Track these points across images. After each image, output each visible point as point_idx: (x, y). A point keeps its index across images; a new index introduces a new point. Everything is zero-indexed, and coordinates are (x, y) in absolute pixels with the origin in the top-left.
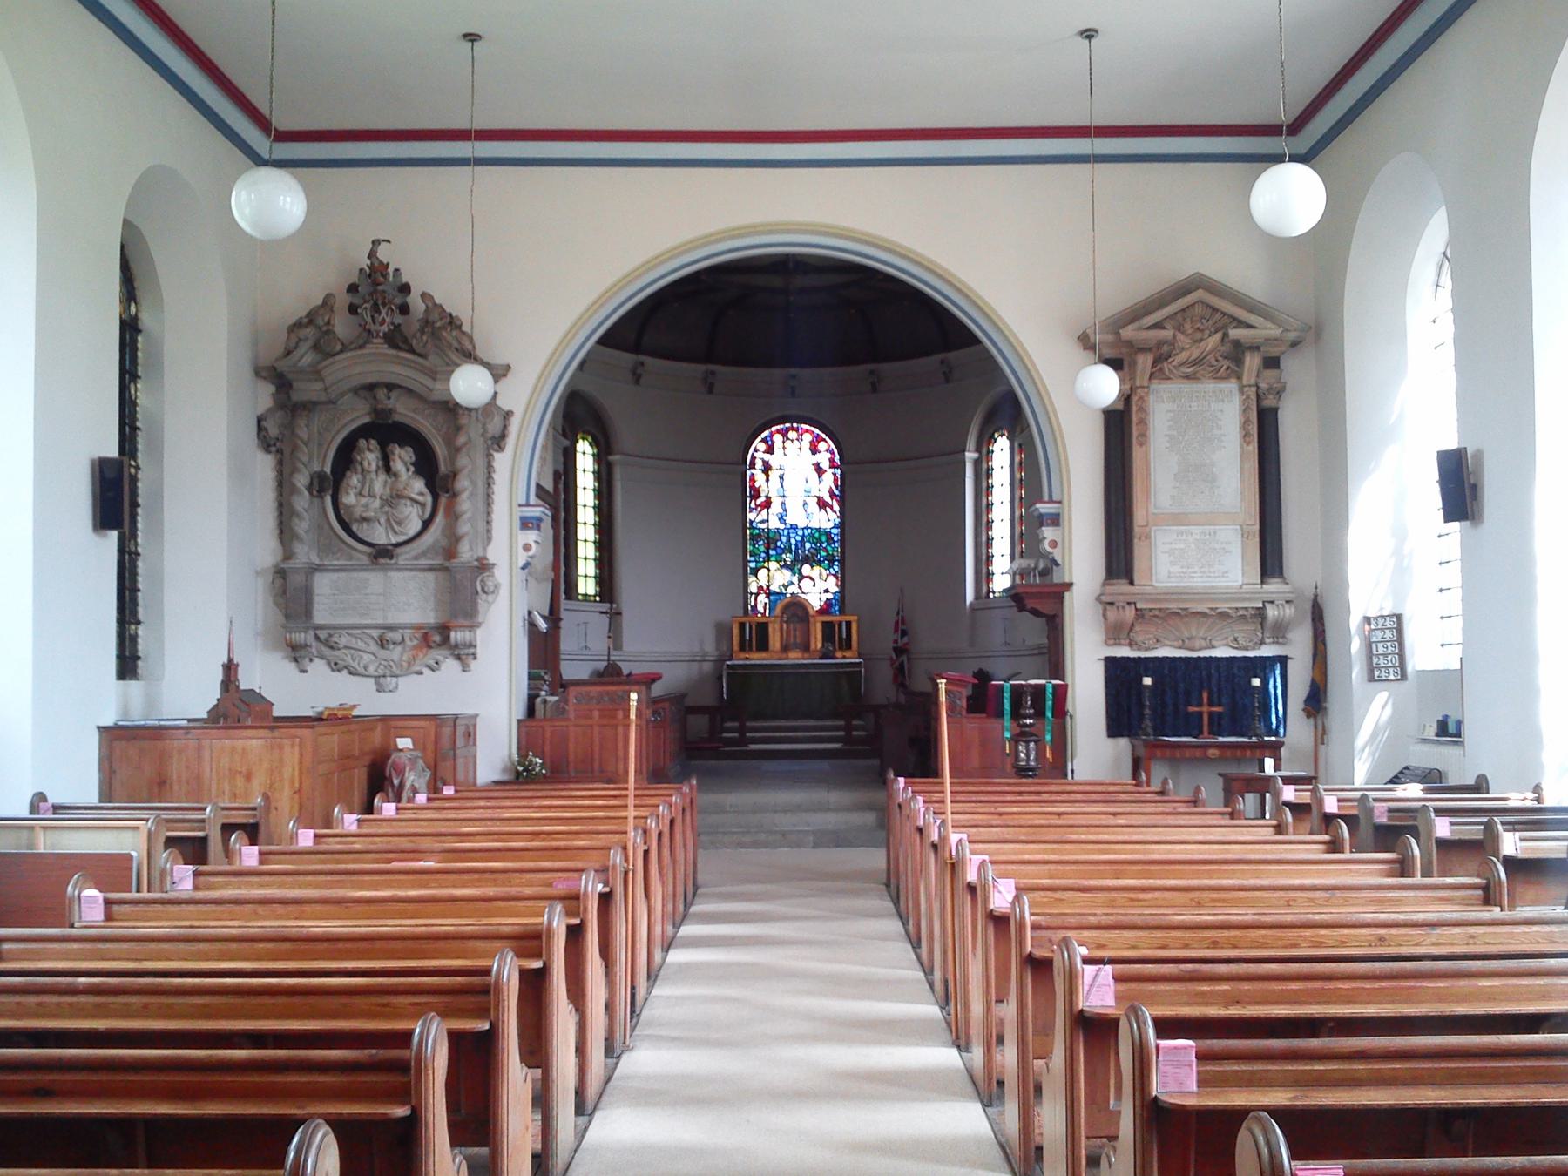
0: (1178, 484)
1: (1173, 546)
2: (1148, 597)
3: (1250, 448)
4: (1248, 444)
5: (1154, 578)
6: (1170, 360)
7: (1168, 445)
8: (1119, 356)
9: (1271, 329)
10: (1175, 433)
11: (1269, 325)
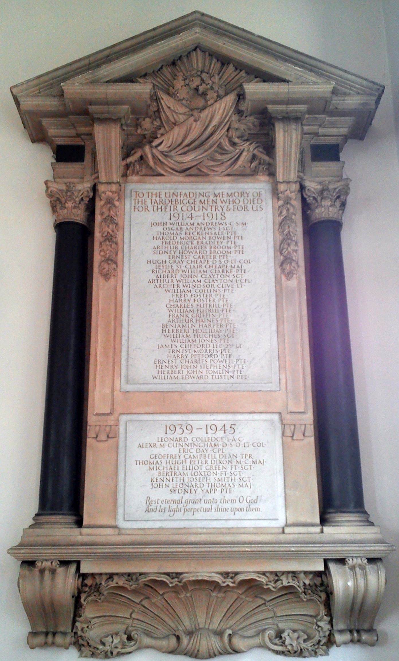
0: (168, 342)
1: (156, 451)
2: (100, 550)
3: (293, 283)
4: (289, 275)
5: (120, 511)
6: (155, 143)
7: (153, 276)
8: (77, 142)
9: (315, 83)
10: (164, 257)
11: (312, 77)
